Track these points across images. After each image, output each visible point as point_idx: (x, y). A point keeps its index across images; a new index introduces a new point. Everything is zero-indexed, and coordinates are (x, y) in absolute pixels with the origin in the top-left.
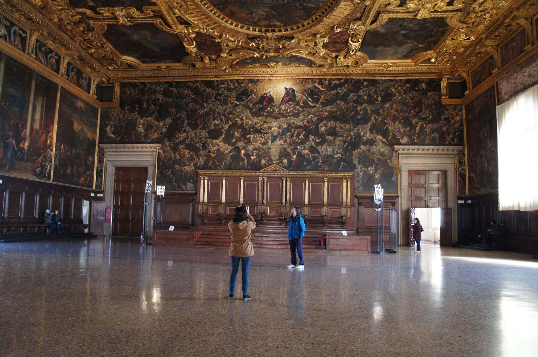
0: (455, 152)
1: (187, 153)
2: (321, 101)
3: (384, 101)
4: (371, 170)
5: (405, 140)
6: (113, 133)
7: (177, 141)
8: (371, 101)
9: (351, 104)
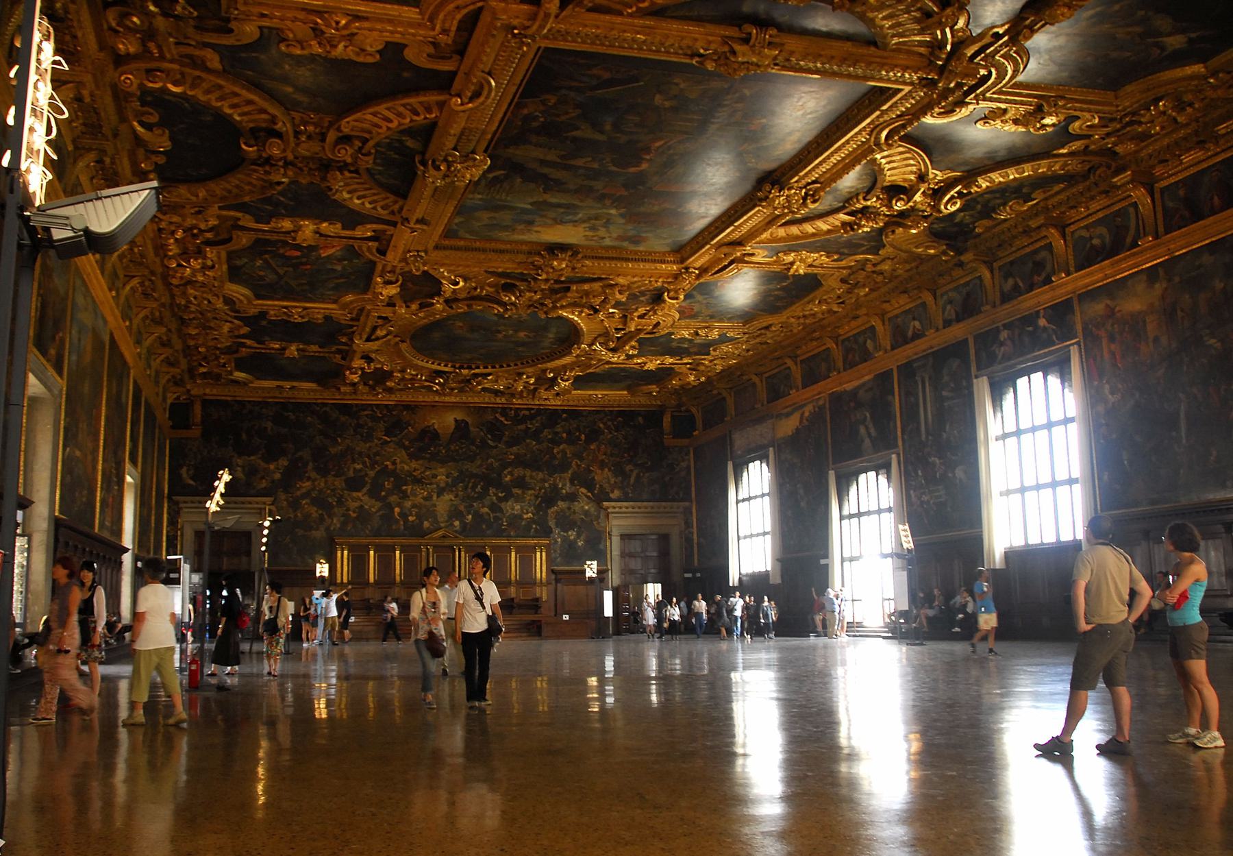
0: (681, 510)
1: (314, 512)
2: (505, 439)
3: (589, 440)
4: (572, 535)
5: (616, 494)
6: (192, 478)
7: (298, 493)
8: (572, 441)
9: (545, 444)
